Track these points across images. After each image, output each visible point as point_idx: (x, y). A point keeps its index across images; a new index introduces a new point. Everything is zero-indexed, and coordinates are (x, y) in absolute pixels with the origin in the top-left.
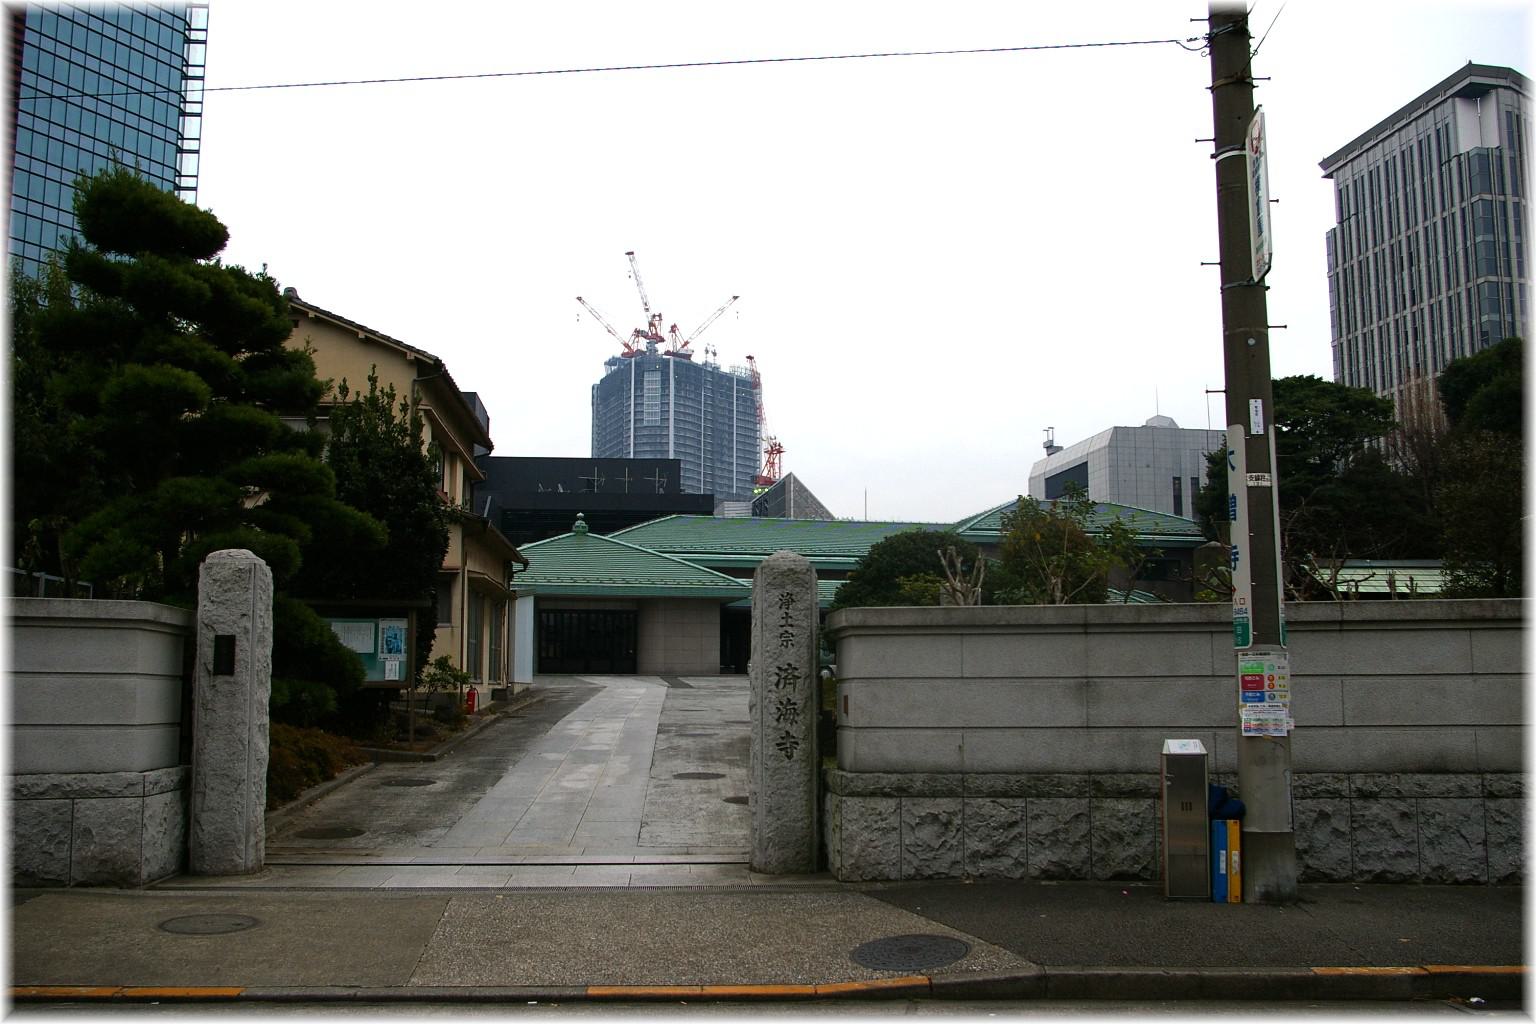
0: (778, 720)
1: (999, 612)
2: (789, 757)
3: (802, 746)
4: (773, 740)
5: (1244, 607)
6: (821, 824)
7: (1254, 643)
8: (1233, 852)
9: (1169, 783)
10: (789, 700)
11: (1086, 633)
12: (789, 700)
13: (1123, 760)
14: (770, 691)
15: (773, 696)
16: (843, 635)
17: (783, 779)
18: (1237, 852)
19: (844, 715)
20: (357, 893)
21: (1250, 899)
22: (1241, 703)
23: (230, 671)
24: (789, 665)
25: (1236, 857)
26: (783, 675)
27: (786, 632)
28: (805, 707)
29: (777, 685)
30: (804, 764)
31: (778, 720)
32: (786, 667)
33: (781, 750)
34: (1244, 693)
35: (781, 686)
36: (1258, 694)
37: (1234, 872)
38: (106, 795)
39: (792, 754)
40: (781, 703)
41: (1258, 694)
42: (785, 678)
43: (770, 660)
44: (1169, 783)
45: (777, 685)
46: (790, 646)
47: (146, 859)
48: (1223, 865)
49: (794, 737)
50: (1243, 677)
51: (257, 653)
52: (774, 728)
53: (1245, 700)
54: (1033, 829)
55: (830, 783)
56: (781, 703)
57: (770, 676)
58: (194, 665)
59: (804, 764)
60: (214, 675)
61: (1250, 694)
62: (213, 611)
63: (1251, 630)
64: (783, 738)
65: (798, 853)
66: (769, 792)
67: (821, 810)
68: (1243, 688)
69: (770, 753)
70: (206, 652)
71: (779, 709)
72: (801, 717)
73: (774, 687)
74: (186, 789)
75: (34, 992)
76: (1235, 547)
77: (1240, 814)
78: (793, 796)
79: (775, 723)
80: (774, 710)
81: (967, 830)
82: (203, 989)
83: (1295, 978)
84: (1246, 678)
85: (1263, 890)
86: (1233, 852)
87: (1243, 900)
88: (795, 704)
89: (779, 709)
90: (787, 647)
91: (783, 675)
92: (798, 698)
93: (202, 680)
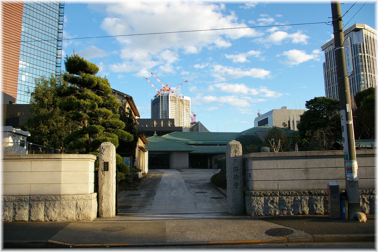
0: (234, 179)
1: (287, 154)
2: (237, 188)
3: (240, 185)
4: (233, 184)
5: (347, 151)
6: (244, 203)
7: (349, 160)
8: (346, 208)
9: (330, 192)
10: (236, 175)
11: (306, 158)
12: (236, 175)
13: (316, 187)
14: (232, 173)
15: (233, 174)
16: (249, 159)
17: (235, 193)
18: (347, 208)
19: (249, 178)
20: (140, 221)
21: (350, 219)
22: (347, 173)
23: (108, 170)
24: (236, 166)
25: (347, 209)
26: (235, 169)
27: (235, 159)
28: (240, 176)
29: (234, 171)
30: (240, 189)
31: (234, 179)
32: (236, 167)
33: (235, 186)
34: (347, 171)
35: (234, 171)
36: (351, 171)
37: (347, 212)
38: (83, 199)
39: (237, 187)
40: (235, 175)
41: (351, 171)
42: (235, 170)
43: (232, 166)
44: (330, 192)
45: (234, 171)
46: (236, 162)
47: (92, 214)
48: (344, 211)
49: (238, 183)
50: (347, 167)
51: (113, 167)
52: (233, 181)
53: (348, 173)
54: (296, 203)
55: (247, 194)
56: (235, 175)
57: (232, 169)
58: (100, 168)
59: (240, 189)
60: (104, 171)
61: (349, 171)
62: (105, 158)
63: (348, 157)
64: (235, 183)
65: (239, 210)
66: (232, 196)
67: (244, 200)
68: (347, 170)
69: (232, 187)
70: (101, 166)
71: (234, 177)
72: (239, 178)
73: (233, 172)
74: (98, 198)
75: (82, 245)
76: (344, 138)
77: (347, 199)
78: (238, 197)
79: (233, 180)
80: (233, 177)
81: (280, 204)
82: (99, 244)
83: (371, 236)
84: (348, 168)
85: (354, 216)
86: (346, 208)
87: (349, 219)
88: (238, 175)
89: (234, 177)
90: (235, 162)
91: (235, 169)
92: (238, 174)
93: (100, 173)
